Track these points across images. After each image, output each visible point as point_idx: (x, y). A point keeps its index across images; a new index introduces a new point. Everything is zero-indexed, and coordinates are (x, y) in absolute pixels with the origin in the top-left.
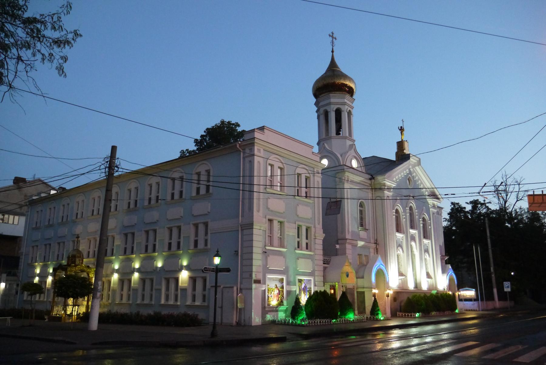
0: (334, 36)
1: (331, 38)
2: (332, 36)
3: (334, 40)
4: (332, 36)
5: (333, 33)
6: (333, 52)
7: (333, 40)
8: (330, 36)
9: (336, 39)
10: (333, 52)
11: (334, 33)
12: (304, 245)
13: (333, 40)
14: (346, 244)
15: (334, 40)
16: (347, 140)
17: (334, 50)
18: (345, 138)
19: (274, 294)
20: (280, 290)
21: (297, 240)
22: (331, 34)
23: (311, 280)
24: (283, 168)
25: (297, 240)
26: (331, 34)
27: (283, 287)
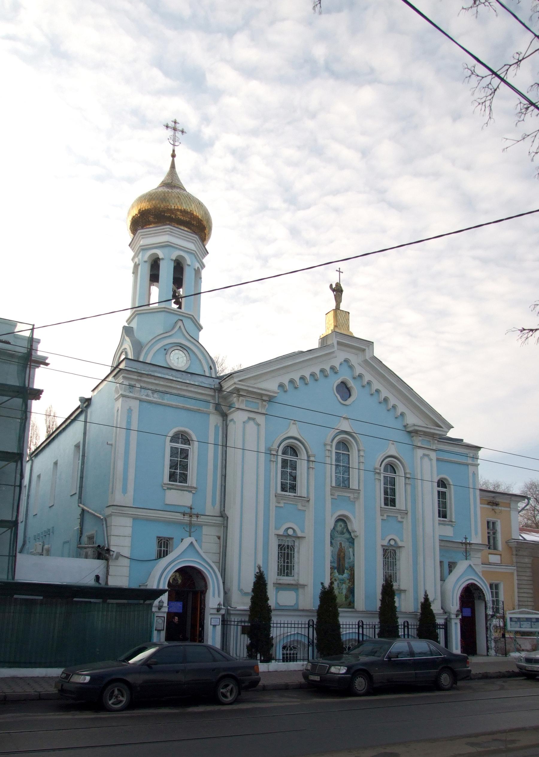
1: (170, 132)
2: (175, 129)
6: (173, 156)
10: (173, 156)
11: (178, 121)
13: (174, 135)
15: (179, 134)
17: (176, 153)
26: (171, 124)
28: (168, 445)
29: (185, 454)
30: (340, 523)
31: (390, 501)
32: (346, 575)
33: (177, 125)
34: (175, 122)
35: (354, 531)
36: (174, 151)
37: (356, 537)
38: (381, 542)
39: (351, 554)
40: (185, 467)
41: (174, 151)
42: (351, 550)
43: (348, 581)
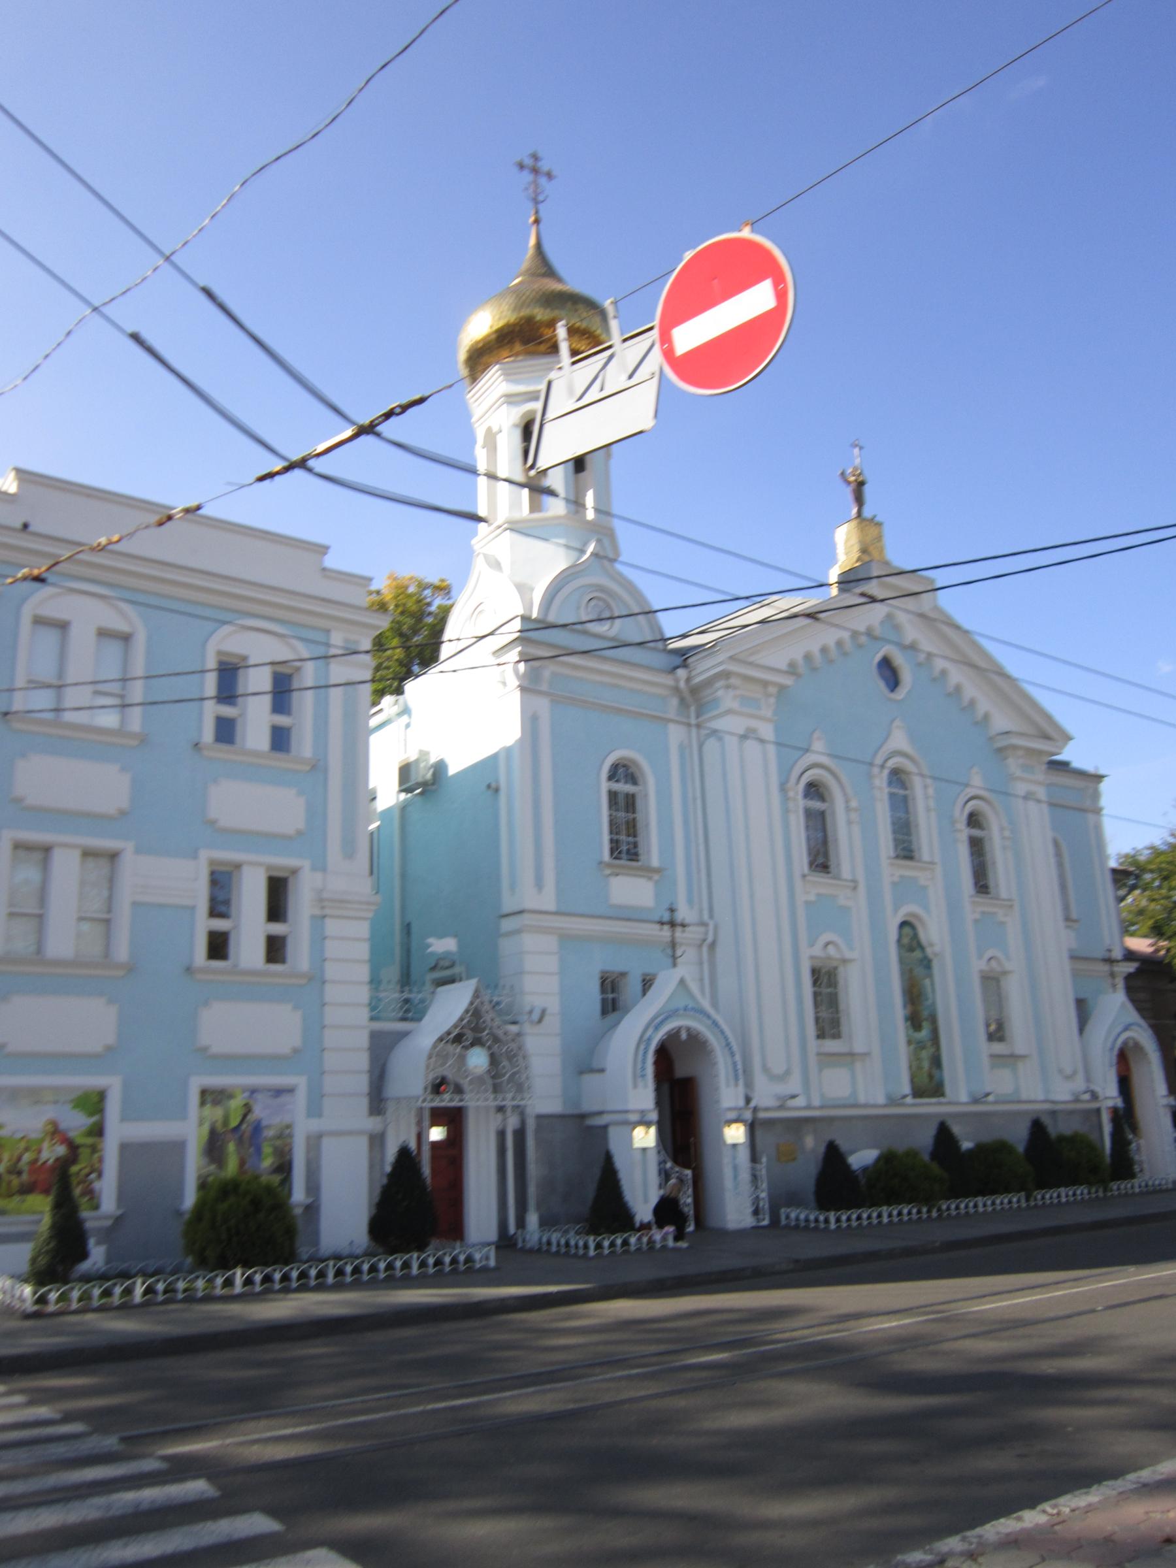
0: (544, 166)
1: (527, 177)
2: (535, 171)
5: (535, 157)
7: (536, 184)
8: (521, 166)
9: (549, 176)
11: (540, 154)
13: (536, 184)
15: (543, 181)
19: (35, 1161)
20: (79, 1140)
22: (529, 162)
23: (290, 1090)
26: (529, 162)
27: (98, 1131)
28: (605, 786)
29: (630, 803)
30: (907, 930)
31: (982, 885)
32: (924, 1034)
33: (540, 164)
35: (931, 945)
37: (936, 955)
38: (978, 965)
39: (929, 989)
40: (632, 828)
42: (927, 982)
43: (929, 1044)
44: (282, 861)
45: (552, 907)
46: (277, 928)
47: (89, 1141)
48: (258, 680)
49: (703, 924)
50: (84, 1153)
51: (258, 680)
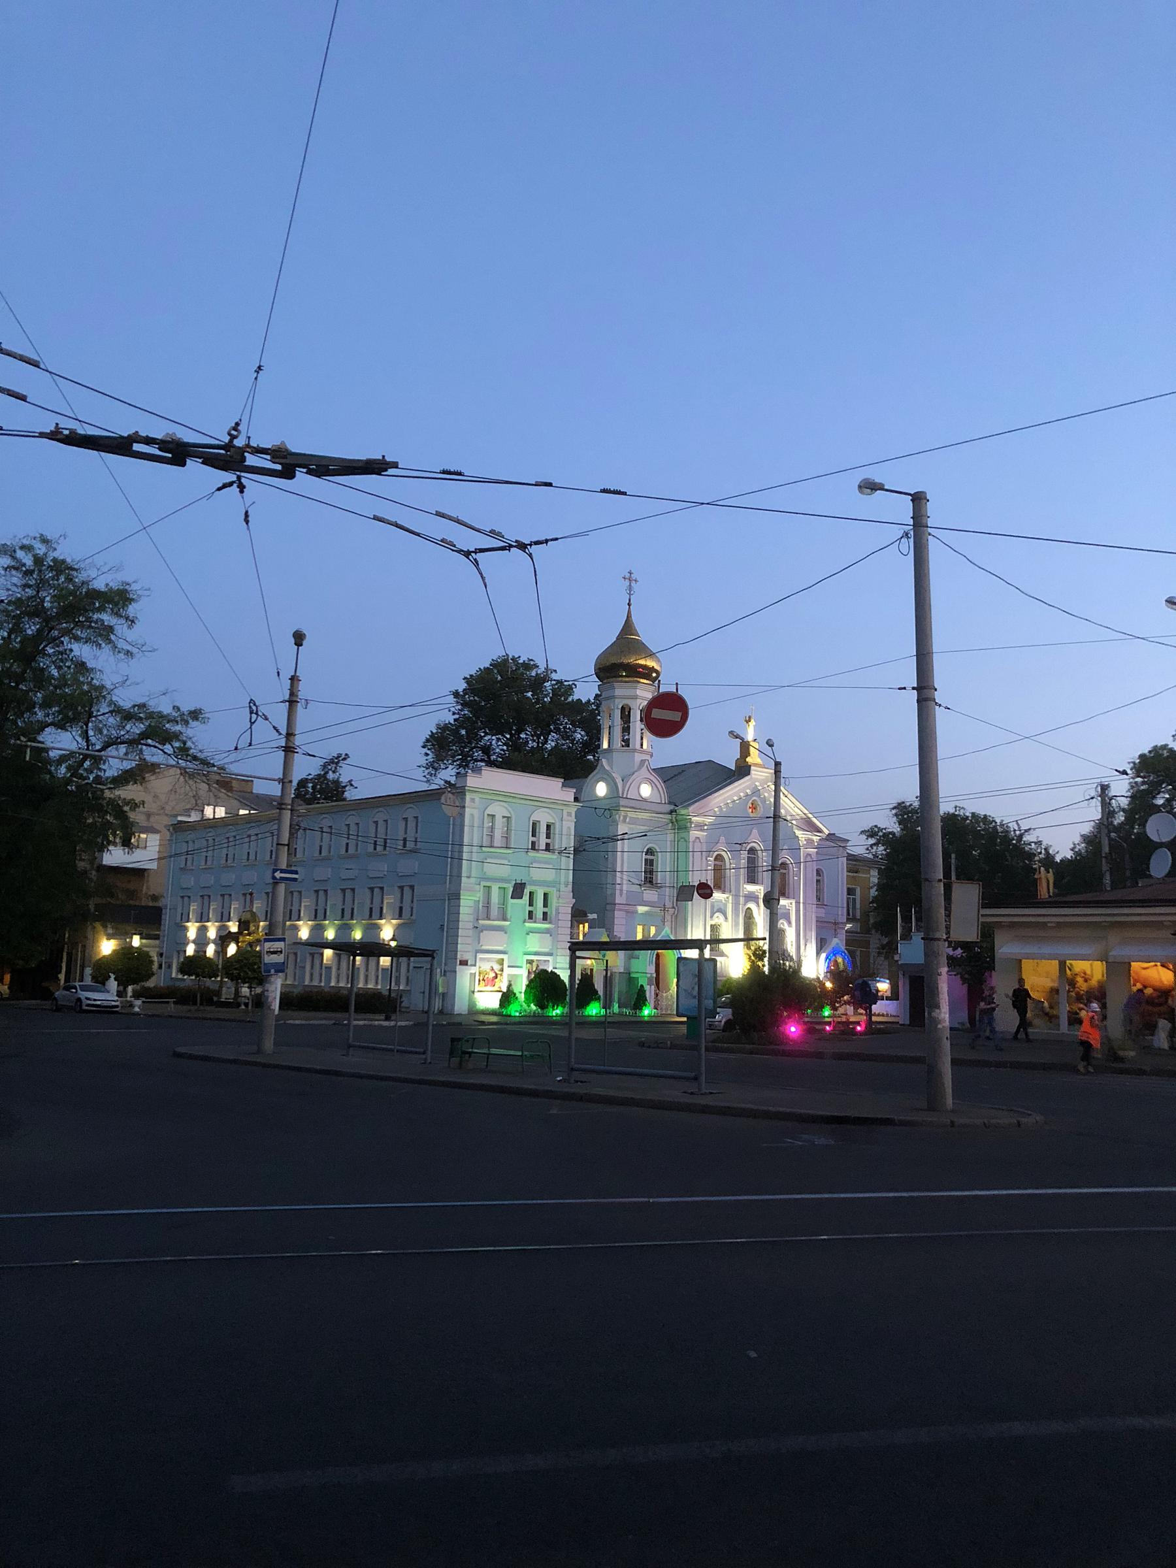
3: (633, 584)
4: (630, 578)
5: (630, 573)
6: (629, 605)
7: (630, 585)
10: (629, 605)
12: (540, 915)
13: (630, 585)
14: (614, 910)
16: (636, 753)
18: (635, 750)
20: (498, 972)
21: (528, 908)
22: (627, 575)
23: (549, 961)
24: (510, 817)
25: (528, 908)
27: (502, 970)
30: (748, 910)
34: (631, 574)
36: (630, 600)
41: (630, 600)
44: (547, 890)
45: (625, 903)
46: (546, 910)
47: (500, 973)
48: (543, 829)
49: (673, 908)
50: (499, 976)
51: (543, 829)
